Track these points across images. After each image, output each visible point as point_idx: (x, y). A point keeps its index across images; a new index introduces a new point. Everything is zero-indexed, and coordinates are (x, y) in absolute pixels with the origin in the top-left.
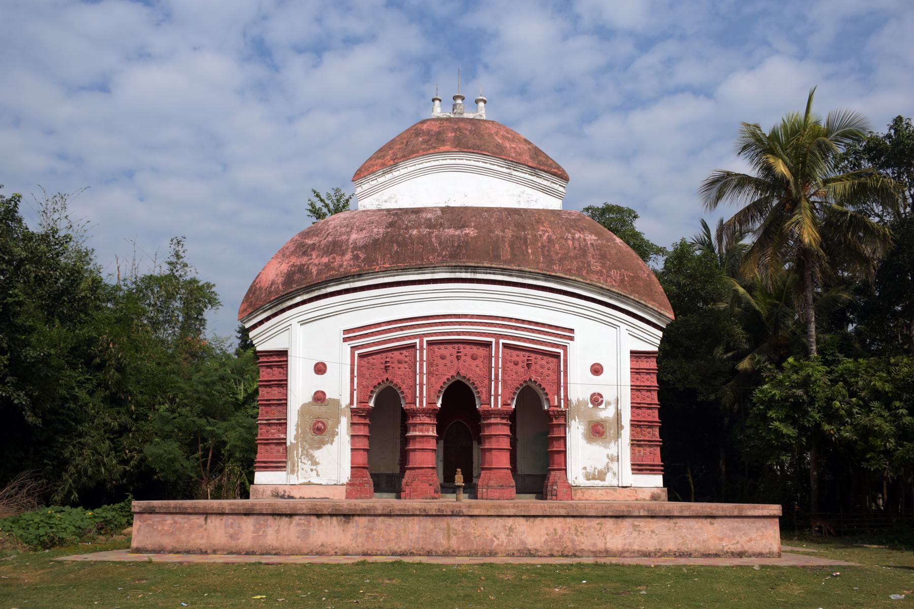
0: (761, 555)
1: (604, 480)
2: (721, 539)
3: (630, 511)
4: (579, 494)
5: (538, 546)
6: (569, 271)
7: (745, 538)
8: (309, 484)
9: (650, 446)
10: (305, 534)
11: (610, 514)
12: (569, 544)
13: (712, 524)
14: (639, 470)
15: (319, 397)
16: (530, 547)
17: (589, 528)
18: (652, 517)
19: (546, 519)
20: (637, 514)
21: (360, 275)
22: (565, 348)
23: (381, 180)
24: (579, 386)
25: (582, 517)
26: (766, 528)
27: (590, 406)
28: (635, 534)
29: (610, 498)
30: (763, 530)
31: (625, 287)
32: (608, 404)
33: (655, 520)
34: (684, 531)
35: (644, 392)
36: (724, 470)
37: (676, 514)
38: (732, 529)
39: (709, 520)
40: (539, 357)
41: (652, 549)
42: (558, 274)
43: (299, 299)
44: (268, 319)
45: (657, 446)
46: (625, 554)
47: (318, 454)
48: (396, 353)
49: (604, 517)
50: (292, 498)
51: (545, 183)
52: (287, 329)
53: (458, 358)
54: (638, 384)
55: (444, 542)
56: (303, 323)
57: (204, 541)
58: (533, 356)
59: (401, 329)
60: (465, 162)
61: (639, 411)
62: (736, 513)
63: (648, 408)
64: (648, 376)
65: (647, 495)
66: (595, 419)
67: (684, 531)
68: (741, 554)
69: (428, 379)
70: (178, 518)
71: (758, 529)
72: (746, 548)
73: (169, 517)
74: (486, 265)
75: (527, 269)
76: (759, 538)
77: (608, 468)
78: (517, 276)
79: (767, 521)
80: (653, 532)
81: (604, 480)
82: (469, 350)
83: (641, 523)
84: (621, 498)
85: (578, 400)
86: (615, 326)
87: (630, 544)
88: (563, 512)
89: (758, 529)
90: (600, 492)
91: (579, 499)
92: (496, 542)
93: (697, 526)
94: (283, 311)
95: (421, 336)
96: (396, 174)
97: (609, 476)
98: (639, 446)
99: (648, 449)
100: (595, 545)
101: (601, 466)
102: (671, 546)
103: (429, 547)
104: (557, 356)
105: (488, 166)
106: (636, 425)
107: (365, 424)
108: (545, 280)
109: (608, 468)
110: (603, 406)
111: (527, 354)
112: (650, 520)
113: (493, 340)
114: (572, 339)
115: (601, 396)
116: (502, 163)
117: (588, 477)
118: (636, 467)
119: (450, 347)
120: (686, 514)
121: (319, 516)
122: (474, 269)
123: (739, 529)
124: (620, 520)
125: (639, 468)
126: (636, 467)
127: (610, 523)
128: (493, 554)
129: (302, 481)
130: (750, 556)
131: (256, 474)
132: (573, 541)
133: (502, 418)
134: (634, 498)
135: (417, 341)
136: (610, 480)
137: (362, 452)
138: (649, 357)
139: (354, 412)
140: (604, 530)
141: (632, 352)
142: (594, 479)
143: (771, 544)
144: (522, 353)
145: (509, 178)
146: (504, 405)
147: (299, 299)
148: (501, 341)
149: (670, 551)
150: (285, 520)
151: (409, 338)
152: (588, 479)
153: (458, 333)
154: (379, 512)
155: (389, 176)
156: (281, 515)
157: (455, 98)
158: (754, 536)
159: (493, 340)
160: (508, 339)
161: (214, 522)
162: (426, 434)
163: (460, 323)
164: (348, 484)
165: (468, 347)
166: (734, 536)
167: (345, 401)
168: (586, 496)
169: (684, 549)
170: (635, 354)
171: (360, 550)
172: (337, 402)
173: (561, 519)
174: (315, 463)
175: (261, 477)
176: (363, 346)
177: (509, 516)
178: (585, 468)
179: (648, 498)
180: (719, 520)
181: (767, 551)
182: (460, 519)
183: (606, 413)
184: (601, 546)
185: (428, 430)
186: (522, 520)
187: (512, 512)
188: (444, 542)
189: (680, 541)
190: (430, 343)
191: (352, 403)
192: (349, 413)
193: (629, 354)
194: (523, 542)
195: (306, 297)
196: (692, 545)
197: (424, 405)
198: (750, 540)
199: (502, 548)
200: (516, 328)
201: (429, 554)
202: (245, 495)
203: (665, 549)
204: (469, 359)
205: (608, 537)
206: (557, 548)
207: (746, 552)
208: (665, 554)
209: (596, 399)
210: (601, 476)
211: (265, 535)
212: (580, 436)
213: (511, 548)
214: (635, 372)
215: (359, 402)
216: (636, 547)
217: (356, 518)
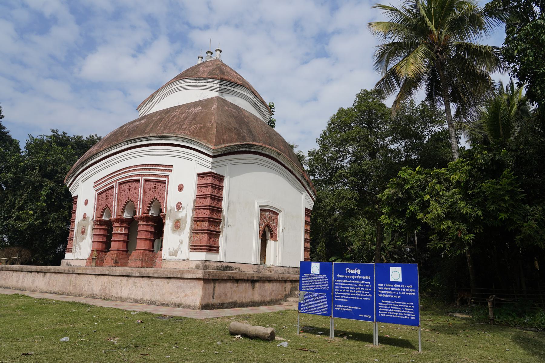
0: (189, 307)
1: (176, 256)
2: (171, 294)
3: (132, 273)
4: (164, 265)
5: (97, 293)
6: (170, 132)
7: (183, 294)
8: (77, 259)
9: (202, 233)
10: (33, 281)
11: (124, 274)
12: (108, 292)
13: (168, 283)
14: (195, 249)
15: (85, 217)
16: (94, 293)
17: (117, 282)
18: (143, 277)
19: (102, 277)
20: (134, 275)
21: (97, 154)
22: (168, 177)
23: (148, 106)
24: (172, 198)
25: (115, 276)
26: (195, 287)
27: (176, 210)
28: (134, 287)
29: (177, 267)
30: (193, 289)
31: (193, 135)
32: (184, 208)
33: (143, 279)
34: (155, 287)
35: (203, 199)
36: (536, 262)
37: (151, 275)
38: (177, 287)
39: (167, 280)
40: (159, 184)
41: (139, 298)
42: (164, 135)
43: (80, 170)
44: (73, 181)
45: (206, 233)
46: (128, 300)
47: (81, 244)
48: (110, 191)
49: (123, 276)
50: (71, 265)
51: (211, 85)
52: (78, 186)
53: (130, 189)
54: (201, 194)
55: (68, 287)
56: (83, 181)
57: (10, 283)
58: (157, 184)
59: (111, 178)
60: (180, 85)
61: (200, 211)
62: (179, 276)
63: (204, 209)
64: (207, 189)
65: (193, 265)
66: (177, 218)
67: (155, 287)
68: (179, 306)
69: (118, 203)
70: (8, 272)
71: (191, 288)
72: (183, 302)
73: (6, 272)
74: (137, 137)
75: (152, 135)
76: (190, 294)
77: (179, 248)
78: (150, 140)
79: (196, 282)
80: (141, 287)
81: (176, 256)
82: (133, 185)
83: (137, 280)
84: (183, 266)
85: (171, 207)
86: (191, 160)
87: (131, 294)
88: (107, 273)
89: (191, 288)
90: (174, 263)
91: (164, 268)
92: (84, 289)
93: (161, 284)
94: (77, 177)
95: (116, 181)
96: (154, 101)
97: (179, 252)
98: (197, 233)
99: (201, 235)
100: (117, 293)
101: (176, 248)
102: (147, 297)
103: (64, 290)
104: (164, 182)
105: (188, 84)
106: (196, 220)
107: (105, 229)
108: (161, 139)
109: (179, 248)
110: (181, 210)
111: (154, 183)
112: (141, 279)
113: (140, 178)
114: (171, 171)
115: (181, 203)
116: (193, 80)
117: (171, 254)
118: (194, 247)
119: (127, 184)
120: (156, 275)
121: (38, 272)
122: (134, 141)
123: (181, 287)
124: (129, 278)
125: (195, 248)
126: (194, 247)
127: (125, 278)
128: (81, 295)
129: (76, 258)
130: (184, 307)
131: (66, 254)
132: (109, 290)
133: (144, 221)
134: (187, 267)
135: (114, 183)
136: (180, 256)
137: (97, 243)
138: (207, 176)
139: (95, 222)
140: (122, 285)
141: (198, 174)
142: (173, 255)
143: (196, 300)
144: (152, 183)
145: (196, 87)
146: (143, 213)
147: (80, 170)
148: (144, 178)
149: (147, 300)
150: (30, 274)
151: (111, 183)
152: (170, 256)
153: (126, 177)
154: (52, 271)
155: (151, 103)
156: (29, 272)
157: (207, 53)
158: (188, 292)
159: (140, 178)
160: (157, 177)
161: (15, 274)
162: (116, 232)
163: (130, 171)
164: (89, 259)
165: (133, 183)
166: (178, 292)
167: (91, 217)
168: (167, 266)
169: (153, 299)
170: (201, 175)
171: (45, 290)
172: (89, 217)
173: (107, 277)
174: (80, 249)
175: (68, 256)
176: (99, 189)
177: (90, 274)
178: (169, 249)
179: (194, 267)
180: (172, 280)
181: (193, 304)
182: (75, 275)
183: (181, 214)
184: (119, 295)
185: (117, 230)
186: (94, 276)
187: (89, 272)
188: (68, 287)
189: (152, 294)
190: (120, 184)
191: (93, 219)
192: (92, 222)
193: (196, 176)
194: (92, 290)
195: (82, 169)
196: (157, 298)
197: (115, 217)
198: (186, 296)
199: (85, 292)
200: (150, 169)
201: (63, 294)
202: (59, 264)
203: (145, 299)
204: (133, 190)
205: (123, 288)
206: (103, 294)
207: (182, 304)
208: (144, 302)
209: (179, 206)
210: (175, 253)
211: (24, 282)
212: (170, 229)
213: (88, 293)
214: (200, 186)
215: (97, 217)
216: (133, 296)
217: (47, 274)
